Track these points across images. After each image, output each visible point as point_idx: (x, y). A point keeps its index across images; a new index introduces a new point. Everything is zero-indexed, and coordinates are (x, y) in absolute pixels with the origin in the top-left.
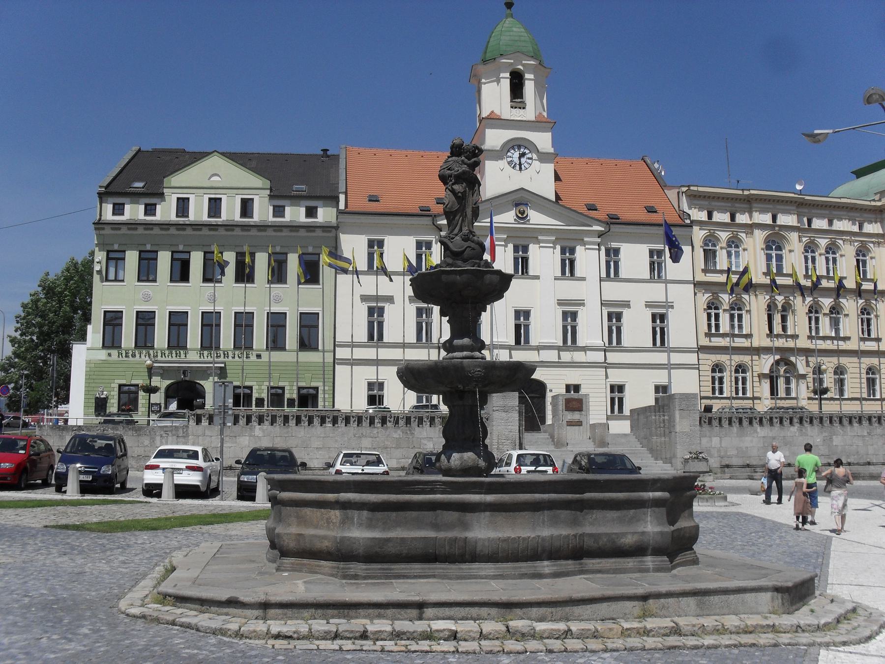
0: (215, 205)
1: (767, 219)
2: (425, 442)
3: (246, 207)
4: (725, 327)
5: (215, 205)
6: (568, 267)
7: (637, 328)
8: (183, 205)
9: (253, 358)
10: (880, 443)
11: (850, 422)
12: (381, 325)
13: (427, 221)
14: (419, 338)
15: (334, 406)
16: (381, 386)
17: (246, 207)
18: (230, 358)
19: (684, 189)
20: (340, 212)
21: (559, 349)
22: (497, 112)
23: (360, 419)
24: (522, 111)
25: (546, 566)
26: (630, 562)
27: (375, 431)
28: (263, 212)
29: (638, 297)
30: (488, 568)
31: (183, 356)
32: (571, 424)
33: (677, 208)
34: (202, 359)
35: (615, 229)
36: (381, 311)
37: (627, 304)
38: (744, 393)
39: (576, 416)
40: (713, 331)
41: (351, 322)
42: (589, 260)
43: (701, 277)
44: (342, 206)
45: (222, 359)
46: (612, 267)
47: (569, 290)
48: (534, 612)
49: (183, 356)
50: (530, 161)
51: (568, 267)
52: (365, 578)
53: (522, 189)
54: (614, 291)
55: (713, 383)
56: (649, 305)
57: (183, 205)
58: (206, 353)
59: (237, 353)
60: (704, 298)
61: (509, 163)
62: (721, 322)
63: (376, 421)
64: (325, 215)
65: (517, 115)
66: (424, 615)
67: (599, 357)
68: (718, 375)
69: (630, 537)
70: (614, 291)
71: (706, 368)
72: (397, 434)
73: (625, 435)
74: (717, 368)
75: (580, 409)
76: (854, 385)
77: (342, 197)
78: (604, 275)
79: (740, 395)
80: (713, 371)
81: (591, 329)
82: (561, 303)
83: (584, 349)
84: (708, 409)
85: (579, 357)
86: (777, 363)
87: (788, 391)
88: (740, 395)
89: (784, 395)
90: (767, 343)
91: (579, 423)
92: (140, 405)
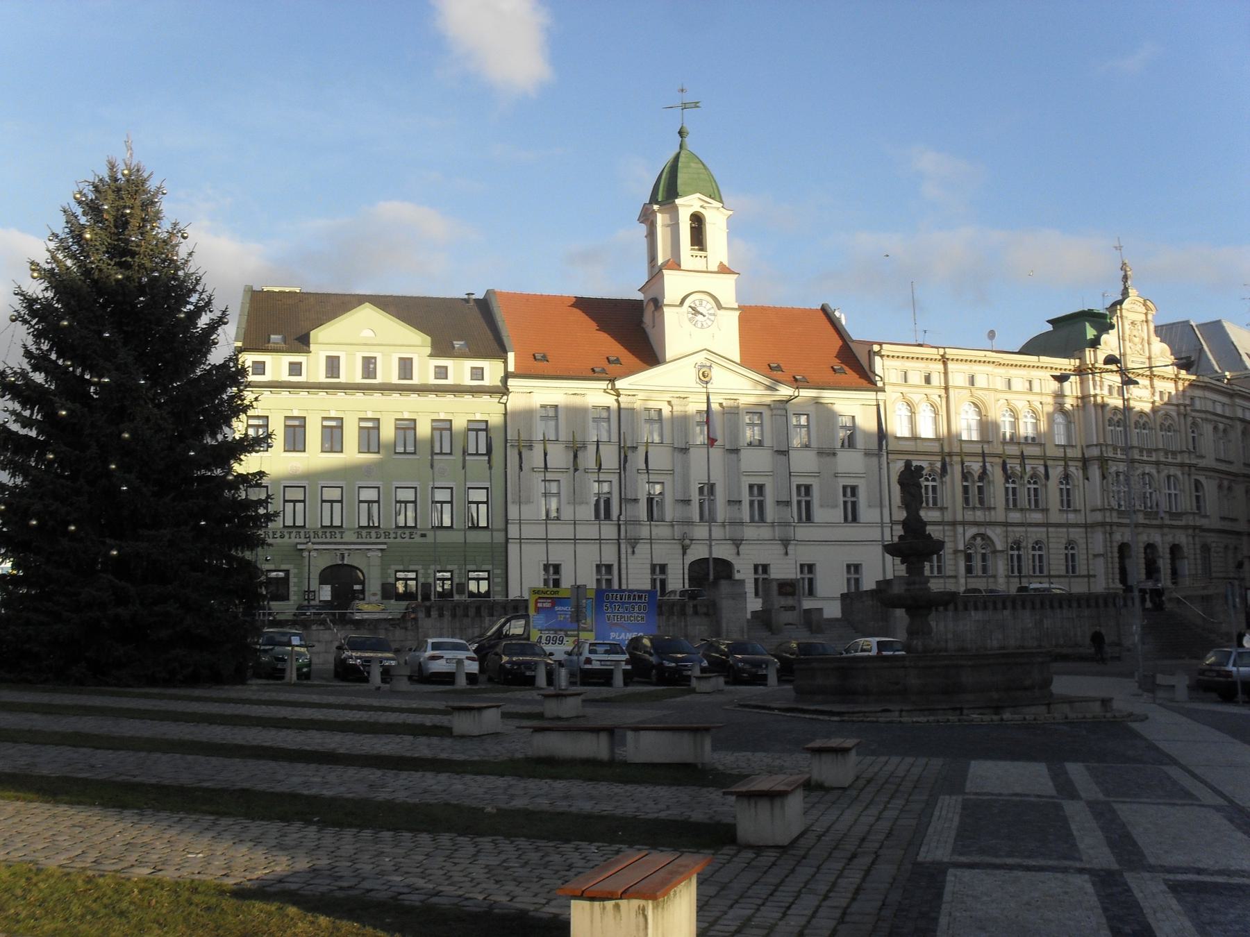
0: (369, 365)
3: (406, 366)
5: (369, 365)
8: (333, 365)
9: (417, 539)
13: (604, 385)
17: (406, 366)
18: (407, 540)
28: (425, 370)
31: (338, 535)
34: (360, 540)
39: (790, 601)
44: (511, 368)
45: (382, 540)
49: (338, 535)
57: (333, 365)
58: (364, 533)
59: (400, 532)
73: (837, 620)
75: (793, 594)
76: (1057, 564)
77: (511, 356)
79: (936, 573)
86: (974, 538)
87: (984, 569)
89: (980, 573)
91: (793, 608)
92: (291, 593)
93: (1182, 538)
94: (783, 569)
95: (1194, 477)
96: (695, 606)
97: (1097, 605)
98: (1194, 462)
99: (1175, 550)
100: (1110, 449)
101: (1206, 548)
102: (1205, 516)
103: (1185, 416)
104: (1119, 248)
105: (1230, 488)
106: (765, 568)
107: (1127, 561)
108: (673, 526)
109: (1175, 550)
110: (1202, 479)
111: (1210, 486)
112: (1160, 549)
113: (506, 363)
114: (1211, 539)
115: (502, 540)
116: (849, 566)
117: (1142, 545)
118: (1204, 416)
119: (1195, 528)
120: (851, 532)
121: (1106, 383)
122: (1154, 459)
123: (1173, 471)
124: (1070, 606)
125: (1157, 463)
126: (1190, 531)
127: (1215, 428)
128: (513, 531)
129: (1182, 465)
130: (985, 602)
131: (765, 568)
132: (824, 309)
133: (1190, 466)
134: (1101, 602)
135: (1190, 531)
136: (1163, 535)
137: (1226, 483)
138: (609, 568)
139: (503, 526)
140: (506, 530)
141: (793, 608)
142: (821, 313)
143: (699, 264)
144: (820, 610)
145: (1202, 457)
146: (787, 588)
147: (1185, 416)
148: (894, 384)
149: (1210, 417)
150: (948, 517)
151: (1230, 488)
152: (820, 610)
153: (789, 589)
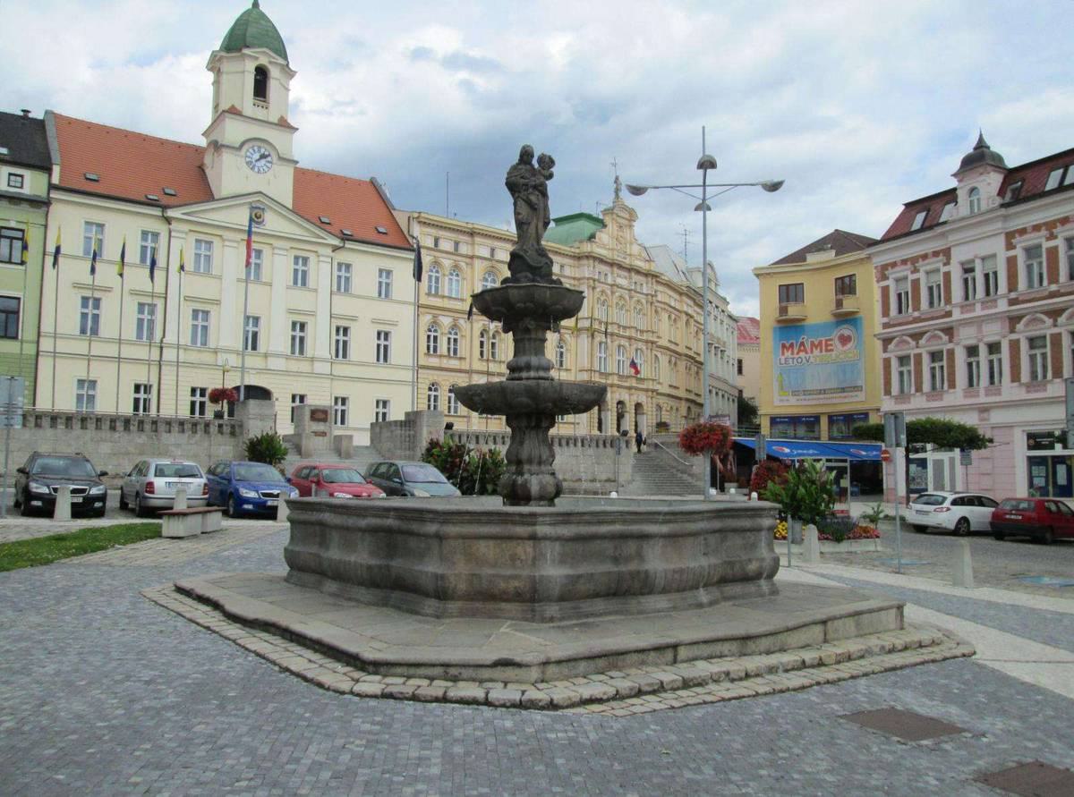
1: (485, 253)
2: (173, 449)
4: (443, 347)
6: (300, 279)
7: (362, 344)
10: (590, 463)
11: (568, 444)
12: (96, 318)
13: (157, 212)
14: (139, 336)
15: (34, 404)
16: (93, 384)
19: (416, 215)
20: (52, 187)
21: (287, 357)
22: (238, 107)
23: (69, 419)
24: (265, 111)
25: (703, 596)
26: (751, 588)
27: (117, 435)
29: (365, 315)
30: (660, 602)
32: (316, 434)
33: (406, 233)
35: (349, 245)
36: (97, 302)
37: (354, 319)
38: (456, 412)
39: (320, 427)
40: (432, 352)
41: (62, 312)
42: (322, 272)
43: (424, 300)
46: (343, 285)
47: (302, 300)
48: (765, 643)
50: (269, 165)
51: (300, 279)
52: (561, 619)
53: (260, 193)
54: (343, 305)
55: (429, 400)
56: (374, 321)
60: (426, 319)
61: (247, 163)
62: (438, 345)
63: (118, 424)
64: (33, 183)
65: (260, 113)
66: (679, 658)
67: (325, 368)
68: (433, 393)
69: (754, 563)
70: (343, 305)
71: (424, 386)
72: (142, 439)
73: (367, 447)
74: (433, 387)
75: (325, 420)
77: (56, 170)
78: (335, 288)
80: (430, 389)
81: (320, 340)
82: (291, 311)
83: (312, 360)
84: (449, 426)
85: (304, 366)
88: (452, 413)
90: (478, 365)
91: (323, 434)
93: (642, 398)
94: (319, 397)
95: (654, 352)
96: (220, 426)
97: (597, 446)
98: (656, 340)
99: (638, 406)
100: (597, 322)
101: (659, 408)
102: (659, 383)
103: (652, 303)
104: (615, 165)
105: (675, 364)
106: (302, 398)
107: (603, 413)
108: (216, 353)
109: (638, 406)
110: (659, 355)
111: (664, 359)
112: (628, 405)
113: (50, 175)
114: (662, 400)
115: (33, 352)
116: (378, 402)
117: (615, 402)
118: (663, 306)
119: (653, 391)
120: (382, 372)
121: (597, 270)
122: (627, 334)
123: (640, 345)
124: (575, 445)
125: (630, 338)
126: (650, 393)
127: (669, 317)
128: (46, 345)
129: (647, 342)
130: (503, 438)
131: (302, 398)
132: (373, 183)
133: (653, 343)
134: (601, 443)
135: (650, 393)
136: (630, 395)
137: (673, 359)
138: (147, 389)
139: (42, 339)
140: (38, 342)
141: (323, 434)
142: (372, 188)
143: (260, 113)
144: (350, 437)
145: (658, 337)
146: (319, 415)
147: (652, 303)
148: (428, 248)
149: (667, 307)
150: (465, 366)
151: (675, 364)
152: (350, 437)
153: (321, 416)
